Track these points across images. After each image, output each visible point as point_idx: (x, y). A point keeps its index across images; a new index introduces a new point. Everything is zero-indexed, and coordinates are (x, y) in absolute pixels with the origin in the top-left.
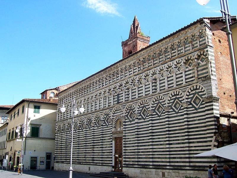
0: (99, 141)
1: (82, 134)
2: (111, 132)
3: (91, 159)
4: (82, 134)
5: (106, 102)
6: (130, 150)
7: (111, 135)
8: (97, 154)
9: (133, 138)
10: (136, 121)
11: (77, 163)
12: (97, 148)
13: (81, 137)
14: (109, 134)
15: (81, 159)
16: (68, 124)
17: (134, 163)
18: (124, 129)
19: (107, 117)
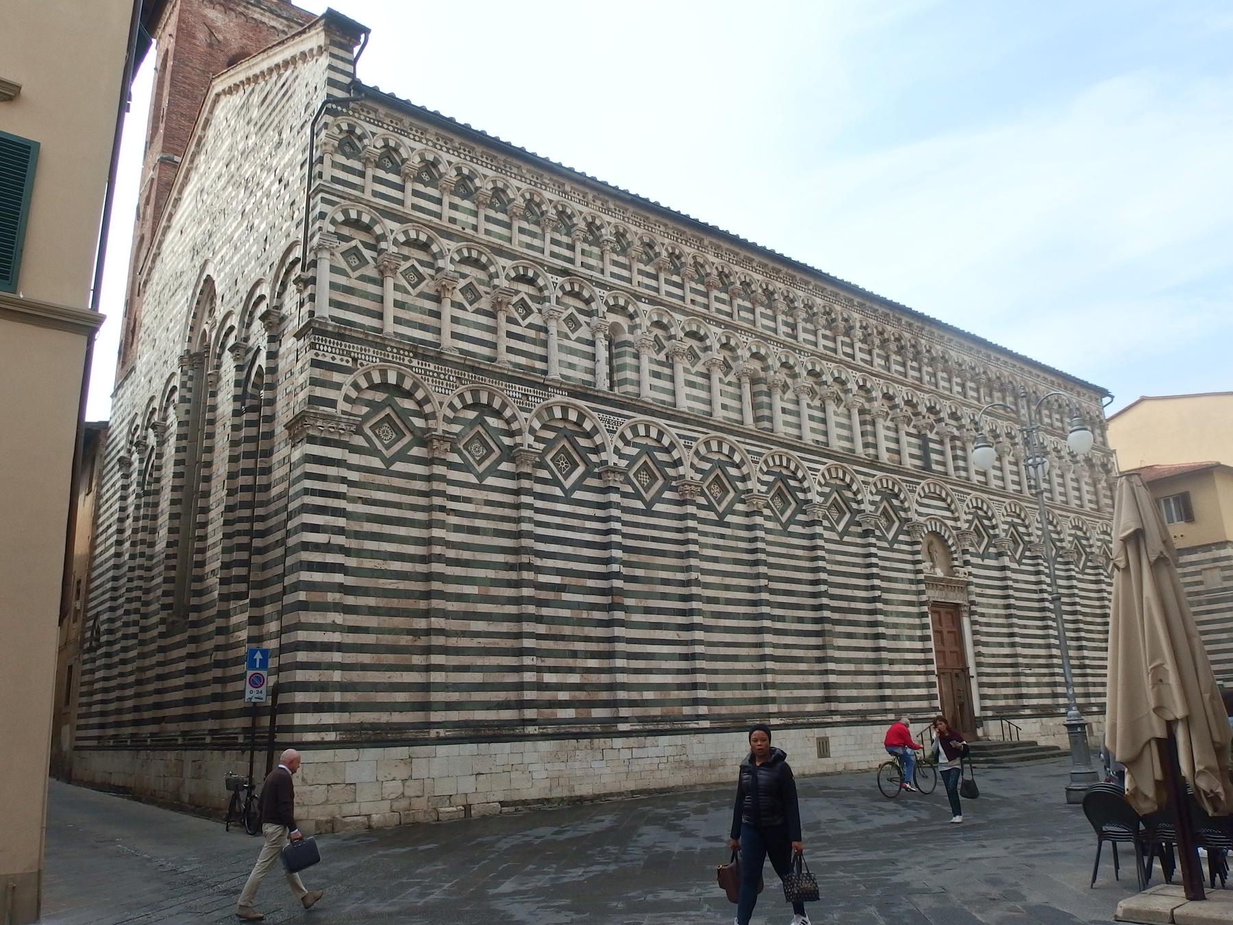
0: (853, 605)
1: (721, 542)
2: (921, 577)
3: (842, 693)
4: (721, 542)
5: (863, 434)
6: (993, 656)
7: (923, 587)
8: (852, 667)
9: (997, 616)
10: (1006, 561)
11: (706, 724)
12: (850, 636)
13: (715, 560)
14: (902, 580)
15: (728, 694)
16: (545, 427)
17: (1011, 702)
18: (971, 579)
19: (881, 501)
